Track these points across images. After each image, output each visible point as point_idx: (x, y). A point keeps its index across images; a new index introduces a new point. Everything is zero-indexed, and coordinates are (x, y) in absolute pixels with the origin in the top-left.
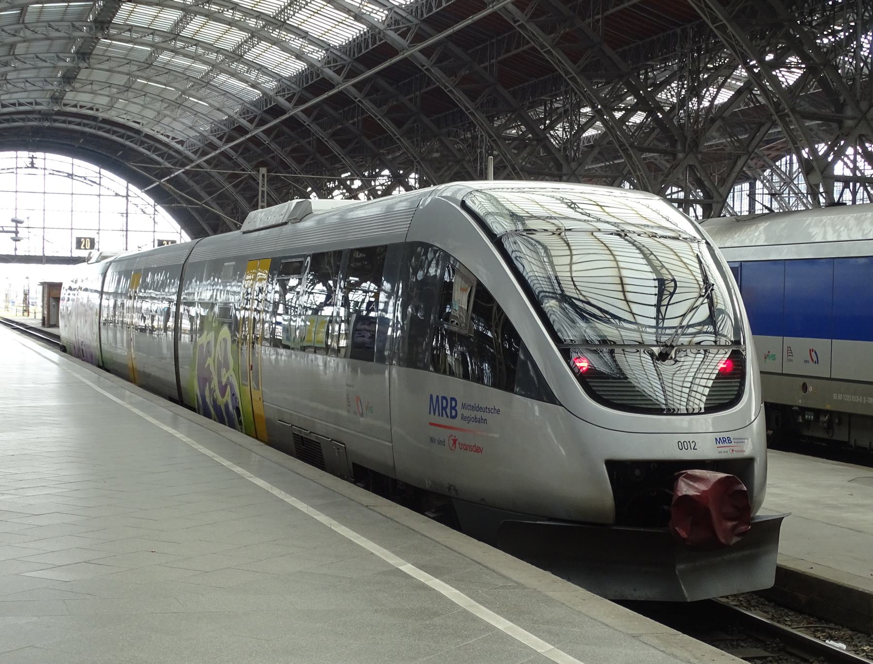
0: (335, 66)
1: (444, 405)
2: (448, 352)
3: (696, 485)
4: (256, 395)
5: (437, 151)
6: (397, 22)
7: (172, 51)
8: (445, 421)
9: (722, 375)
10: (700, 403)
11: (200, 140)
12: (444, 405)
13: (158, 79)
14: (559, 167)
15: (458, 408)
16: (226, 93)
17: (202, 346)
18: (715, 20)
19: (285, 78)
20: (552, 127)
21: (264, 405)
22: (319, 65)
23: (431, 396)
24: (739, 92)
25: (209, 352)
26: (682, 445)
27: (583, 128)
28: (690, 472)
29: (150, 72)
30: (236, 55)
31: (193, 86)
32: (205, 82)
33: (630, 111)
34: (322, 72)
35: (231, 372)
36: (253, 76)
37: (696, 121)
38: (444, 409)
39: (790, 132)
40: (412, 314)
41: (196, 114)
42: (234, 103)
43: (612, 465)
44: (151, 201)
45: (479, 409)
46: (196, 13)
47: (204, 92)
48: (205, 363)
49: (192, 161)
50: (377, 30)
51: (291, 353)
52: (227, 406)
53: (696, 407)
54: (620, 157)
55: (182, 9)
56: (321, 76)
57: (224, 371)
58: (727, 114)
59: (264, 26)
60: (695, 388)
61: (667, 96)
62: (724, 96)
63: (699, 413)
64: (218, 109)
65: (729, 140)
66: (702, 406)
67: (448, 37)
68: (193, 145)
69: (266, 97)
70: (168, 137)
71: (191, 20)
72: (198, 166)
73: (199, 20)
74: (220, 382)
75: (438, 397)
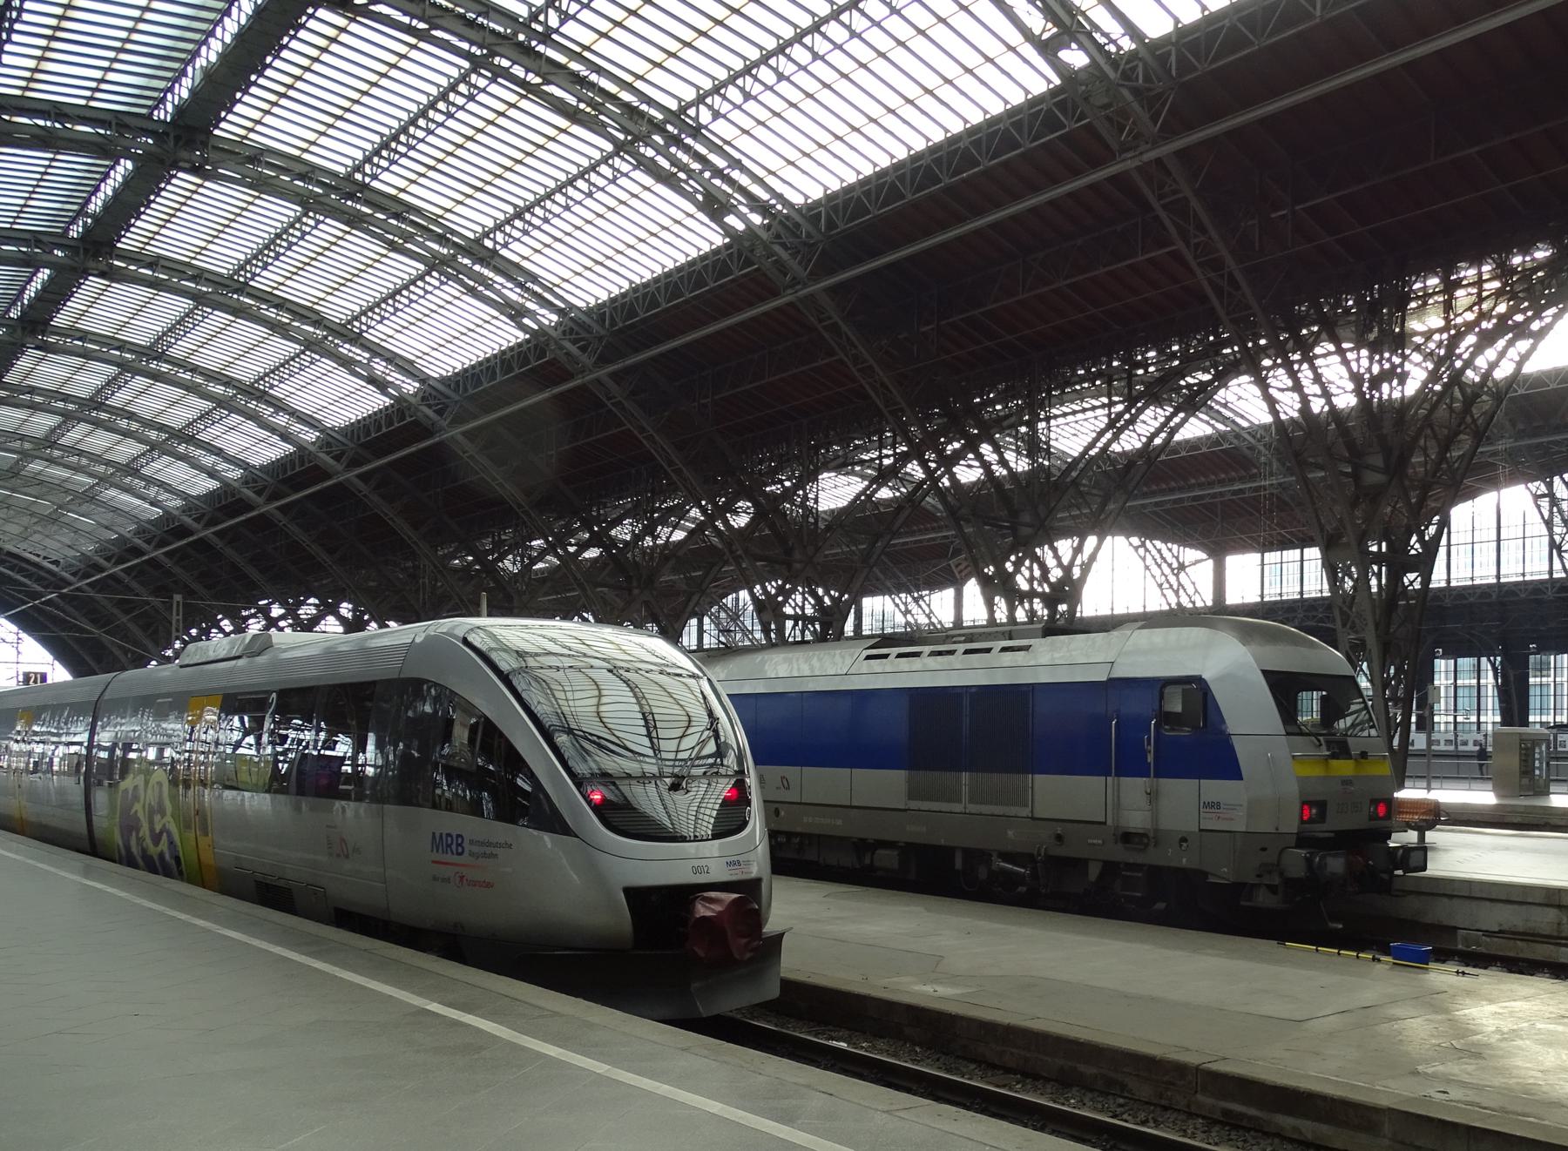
0: (254, 487)
1: (449, 842)
2: (446, 788)
3: (712, 906)
4: (203, 842)
5: (374, 581)
6: (329, 444)
7: (47, 460)
8: (449, 858)
9: (726, 803)
10: (707, 828)
11: (80, 561)
12: (449, 842)
13: (26, 490)
14: (509, 598)
15: (466, 844)
16: (115, 510)
17: (126, 791)
18: (671, 463)
19: (192, 497)
20: (501, 558)
21: (214, 853)
22: (236, 485)
23: (434, 833)
24: (691, 533)
25: (136, 798)
26: (696, 870)
27: (534, 561)
28: (706, 894)
29: (16, 482)
30: (131, 469)
31: (72, 500)
32: (89, 497)
33: (583, 546)
34: (239, 492)
35: (168, 818)
36: (152, 492)
37: (652, 558)
38: (449, 846)
39: (742, 571)
40: (403, 751)
41: (76, 531)
42: (126, 521)
43: (630, 892)
44: (14, 628)
45: (489, 844)
46: (80, 420)
47: (85, 507)
48: (131, 808)
49: (70, 584)
50: (307, 452)
51: (253, 796)
52: (161, 855)
53: (703, 833)
54: (574, 590)
55: (62, 415)
56: (237, 497)
57: (157, 818)
58: (680, 553)
59: (167, 439)
60: (701, 816)
61: (623, 533)
62: (679, 535)
63: (690, 841)
64: (106, 528)
65: (682, 576)
66: (710, 833)
67: (390, 464)
68: (71, 565)
69: (168, 516)
70: (38, 556)
71: (73, 427)
72: (78, 589)
73: (83, 428)
74: (152, 830)
75: (441, 834)
